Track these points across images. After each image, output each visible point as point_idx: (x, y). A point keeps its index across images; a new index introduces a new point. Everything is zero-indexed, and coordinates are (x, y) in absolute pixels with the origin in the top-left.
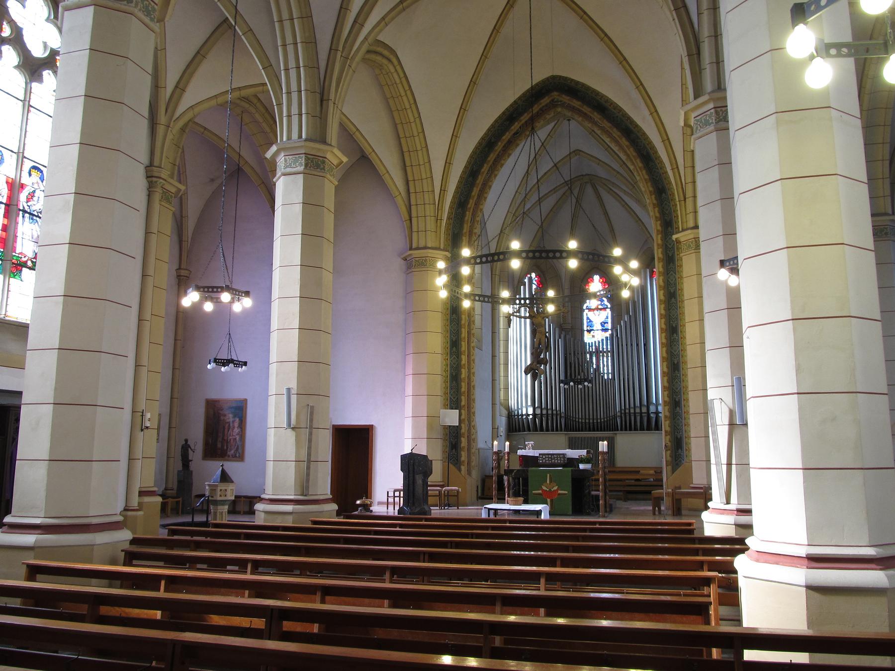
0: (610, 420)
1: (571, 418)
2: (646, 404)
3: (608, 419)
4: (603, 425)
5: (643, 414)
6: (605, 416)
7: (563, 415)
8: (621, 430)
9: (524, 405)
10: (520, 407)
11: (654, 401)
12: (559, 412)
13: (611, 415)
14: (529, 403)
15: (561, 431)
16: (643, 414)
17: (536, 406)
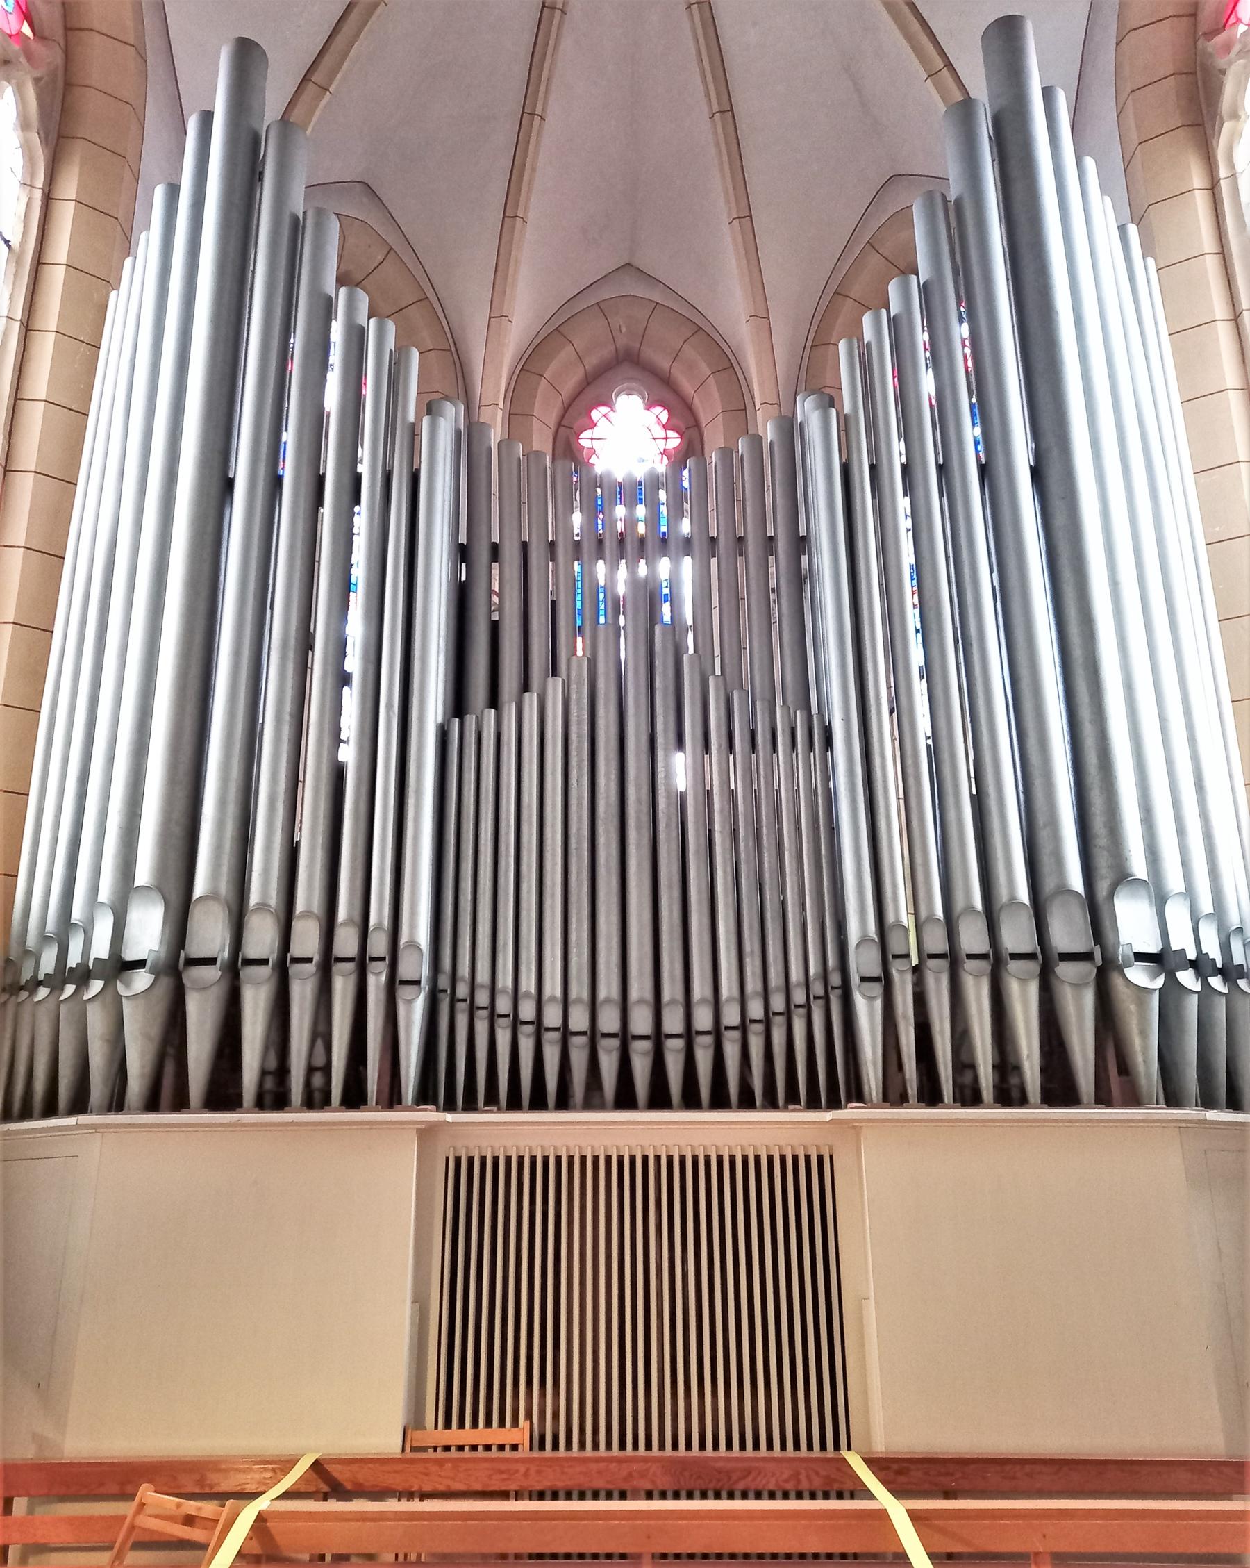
0: (788, 1014)
1: (482, 998)
2: (1076, 881)
3: (778, 1003)
4: (731, 1052)
5: (1065, 971)
6: (753, 984)
7: (416, 965)
8: (894, 1095)
9: (104, 894)
10: (77, 914)
11: (1138, 867)
12: (379, 945)
13: (796, 974)
14: (144, 874)
15: (392, 1099)
16: (1065, 971)
17: (199, 889)
